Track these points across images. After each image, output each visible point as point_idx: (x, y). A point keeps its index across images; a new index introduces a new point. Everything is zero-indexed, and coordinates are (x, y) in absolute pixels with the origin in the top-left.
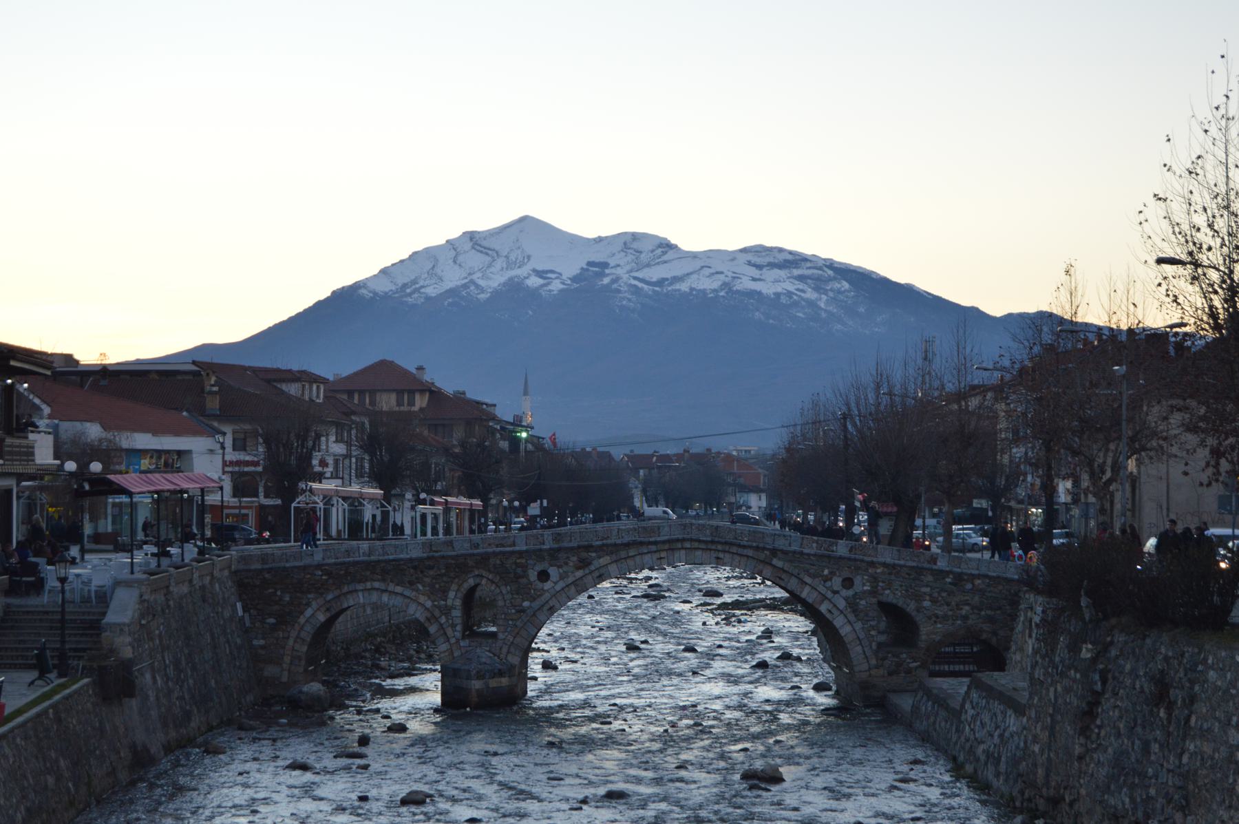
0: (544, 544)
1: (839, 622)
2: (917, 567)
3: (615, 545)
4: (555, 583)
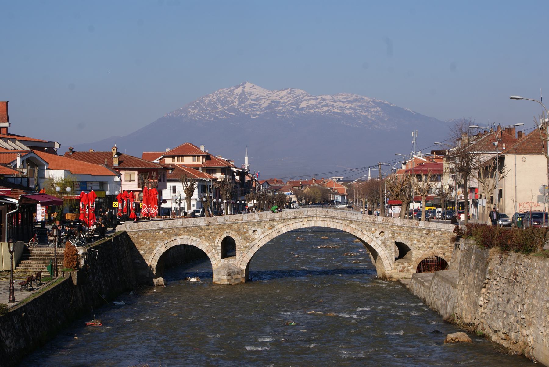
1: (378, 250)
2: (411, 227)
4: (260, 235)
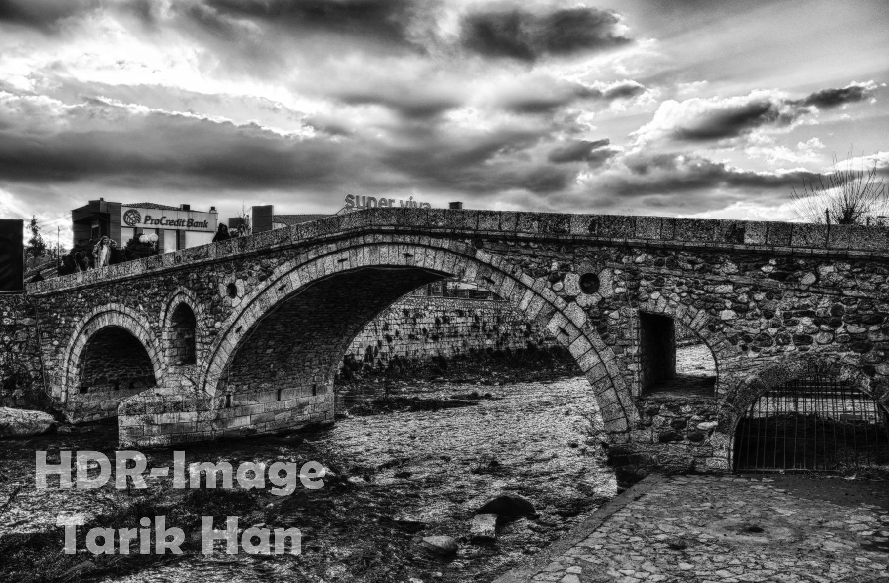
0: (230, 252)
3: (294, 247)
4: (241, 299)
